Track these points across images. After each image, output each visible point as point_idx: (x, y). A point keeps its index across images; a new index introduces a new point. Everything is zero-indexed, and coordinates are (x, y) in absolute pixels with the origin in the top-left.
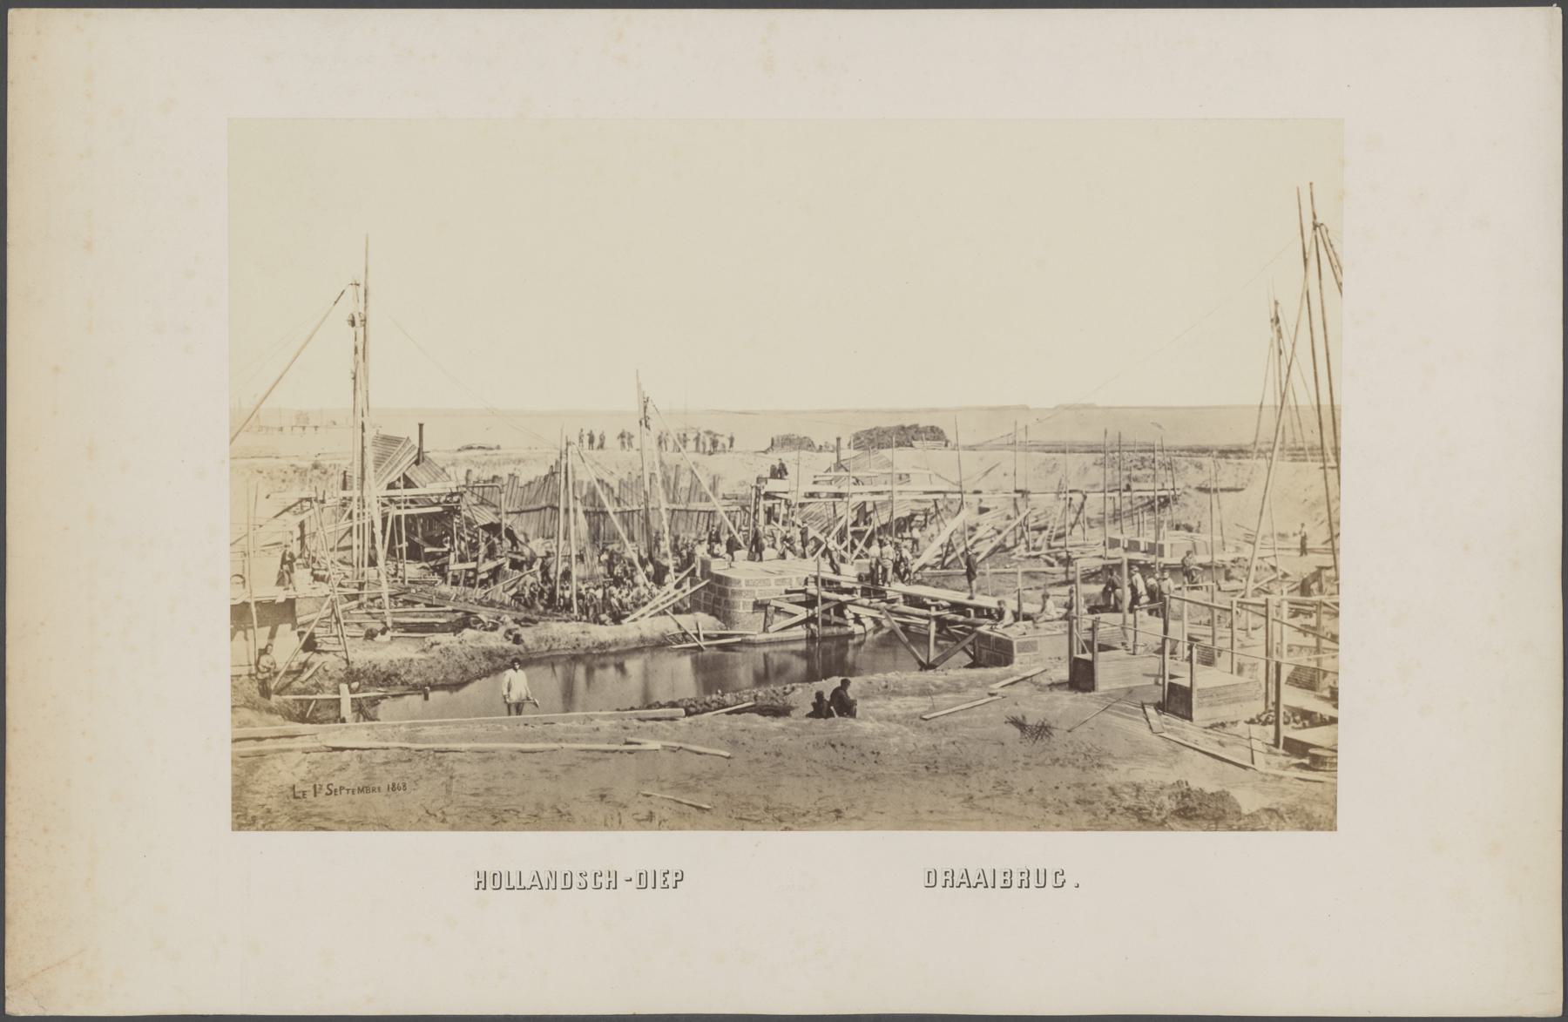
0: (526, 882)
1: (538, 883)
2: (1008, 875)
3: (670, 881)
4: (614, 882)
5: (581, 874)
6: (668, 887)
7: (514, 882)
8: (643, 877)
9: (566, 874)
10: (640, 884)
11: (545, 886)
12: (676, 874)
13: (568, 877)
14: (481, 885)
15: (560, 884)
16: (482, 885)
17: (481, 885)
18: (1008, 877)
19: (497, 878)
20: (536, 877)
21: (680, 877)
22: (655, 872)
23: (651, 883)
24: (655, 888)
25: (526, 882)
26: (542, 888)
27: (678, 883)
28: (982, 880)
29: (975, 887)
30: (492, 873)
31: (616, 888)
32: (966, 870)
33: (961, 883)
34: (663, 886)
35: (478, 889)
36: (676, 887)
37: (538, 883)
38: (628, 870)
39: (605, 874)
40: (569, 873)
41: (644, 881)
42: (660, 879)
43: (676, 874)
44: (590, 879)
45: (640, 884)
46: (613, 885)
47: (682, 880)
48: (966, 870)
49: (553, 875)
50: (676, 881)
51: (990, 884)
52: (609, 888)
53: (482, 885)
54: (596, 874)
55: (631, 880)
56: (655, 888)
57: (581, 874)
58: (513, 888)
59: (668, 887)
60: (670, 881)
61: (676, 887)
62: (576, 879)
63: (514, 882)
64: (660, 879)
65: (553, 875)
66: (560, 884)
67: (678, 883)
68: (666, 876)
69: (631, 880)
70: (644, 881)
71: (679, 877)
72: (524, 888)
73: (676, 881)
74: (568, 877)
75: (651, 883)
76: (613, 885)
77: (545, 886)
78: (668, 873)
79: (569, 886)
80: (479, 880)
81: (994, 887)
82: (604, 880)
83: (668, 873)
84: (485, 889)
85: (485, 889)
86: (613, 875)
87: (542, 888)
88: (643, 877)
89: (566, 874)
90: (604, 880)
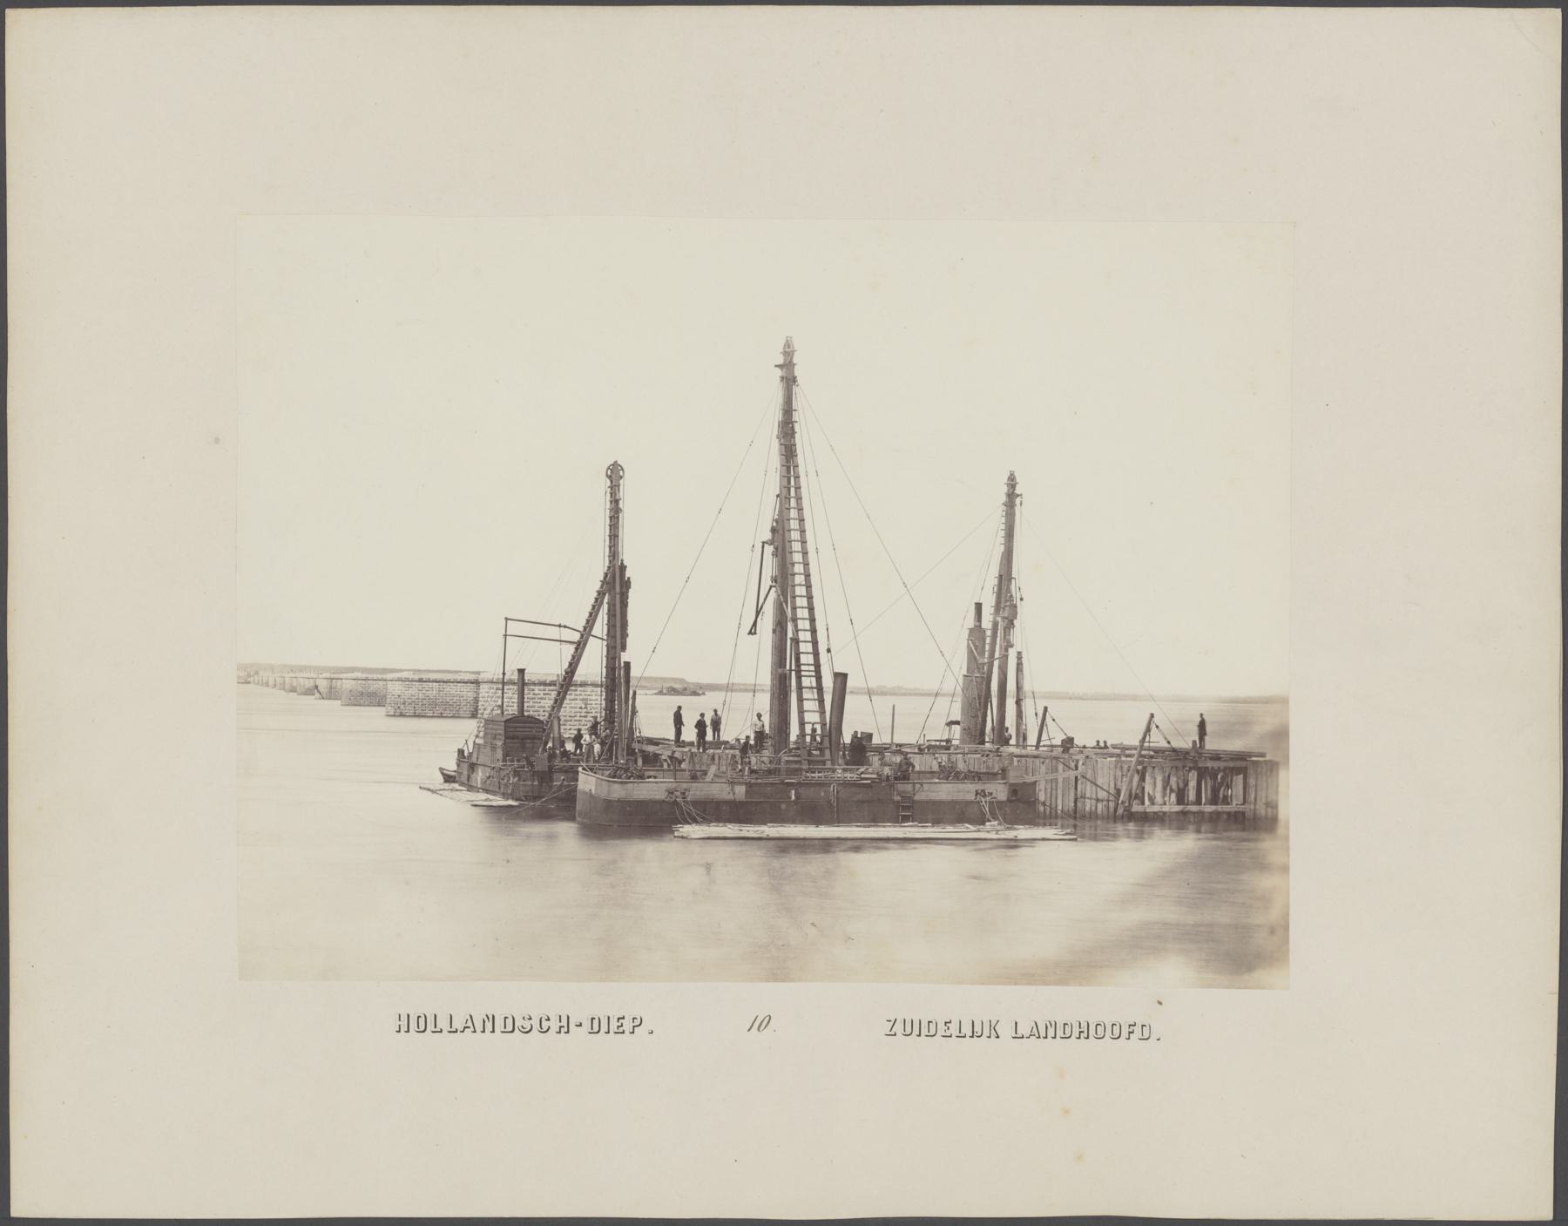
23: (604, 1028)
41: (596, 1026)
45: (592, 1029)
55: (581, 1025)
69: (581, 1025)
70: (596, 1026)
75: (604, 1028)
88: (596, 1023)
90: (554, 1024)
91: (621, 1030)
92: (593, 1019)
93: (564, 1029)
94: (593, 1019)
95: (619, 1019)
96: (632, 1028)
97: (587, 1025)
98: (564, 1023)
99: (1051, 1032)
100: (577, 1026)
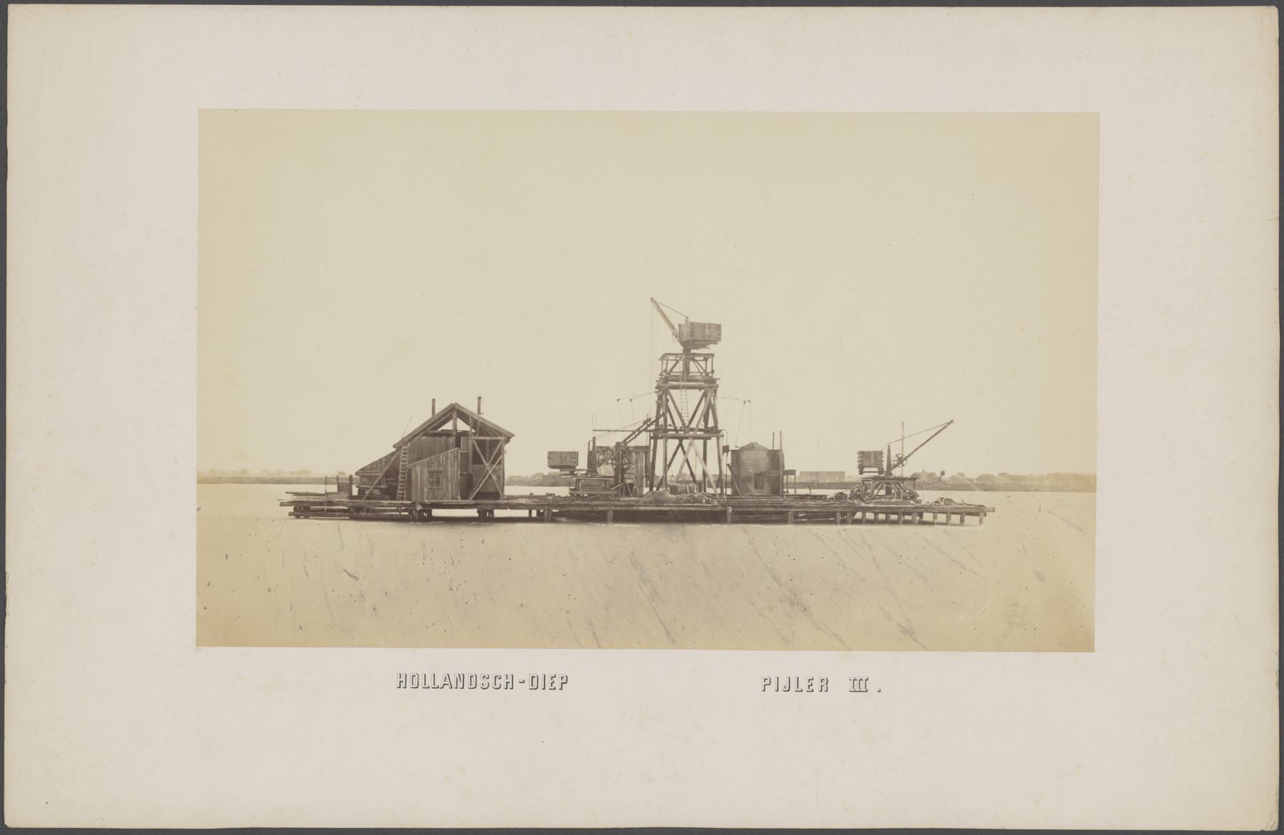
2: (825, 682)
3: (557, 685)
7: (429, 682)
9: (471, 676)
11: (454, 685)
13: (474, 679)
14: (401, 684)
16: (403, 685)
17: (401, 684)
23: (541, 685)
24: (544, 689)
25: (439, 682)
26: (452, 688)
27: (563, 685)
33: (444, 685)
37: (448, 683)
38: (522, 674)
39: (504, 678)
41: (534, 684)
44: (491, 681)
47: (566, 683)
50: (562, 683)
51: (454, 685)
52: (507, 688)
53: (403, 685)
55: (524, 682)
56: (544, 689)
59: (555, 689)
60: (557, 684)
61: (561, 689)
63: (429, 682)
65: (461, 678)
67: (563, 685)
69: (524, 682)
70: (534, 684)
73: (562, 683)
74: (474, 679)
75: (541, 685)
76: (510, 686)
78: (555, 677)
83: (555, 677)
86: (510, 678)
87: (452, 688)
88: (535, 680)
90: (503, 682)
92: (533, 677)
93: (510, 685)
94: (533, 677)
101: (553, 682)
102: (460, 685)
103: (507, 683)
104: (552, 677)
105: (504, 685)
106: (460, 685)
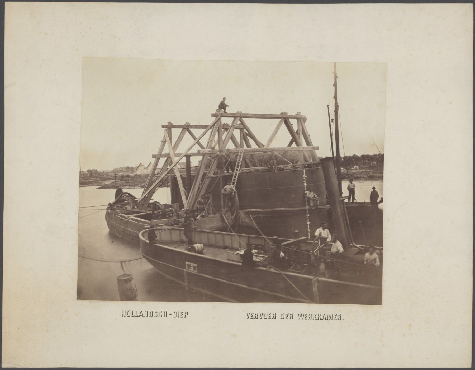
0: (138, 314)
1: (142, 315)
3: (184, 314)
4: (166, 315)
5: (155, 312)
6: (183, 317)
7: (134, 314)
8: (175, 314)
9: (151, 312)
10: (174, 316)
11: (144, 316)
12: (186, 313)
13: (151, 313)
15: (149, 315)
18: (340, 317)
19: (129, 313)
20: (141, 313)
21: (187, 314)
22: (179, 312)
23: (177, 316)
25: (138, 314)
26: (143, 316)
28: (324, 318)
29: (139, 316)
30: (174, 312)
31: (166, 317)
32: (142, 311)
34: (181, 317)
35: (123, 316)
36: (185, 317)
37: (142, 315)
38: (170, 311)
39: (163, 312)
40: (152, 312)
41: (175, 315)
42: (180, 314)
43: (186, 313)
44: (158, 314)
45: (174, 316)
46: (165, 316)
47: (187, 315)
48: (142, 311)
49: (147, 312)
50: (186, 315)
52: (164, 317)
54: (160, 312)
55: (171, 314)
56: (179, 317)
57: (155, 312)
58: (134, 316)
59: (183, 317)
60: (184, 314)
61: (185, 317)
62: (154, 314)
63: (134, 314)
64: (180, 314)
65: (147, 312)
66: (149, 315)
68: (182, 313)
70: (175, 315)
71: (187, 314)
72: (137, 316)
73: (186, 315)
74: (151, 313)
75: (177, 316)
76: (165, 316)
77: (327, 319)
79: (151, 316)
80: (165, 314)
81: (145, 317)
82: (163, 314)
83: (183, 312)
84: (125, 316)
85: (125, 316)
86: (165, 313)
87: (143, 316)
88: (175, 314)
89: (151, 312)
90: (163, 314)
91: (252, 318)
92: (174, 313)
93: (166, 316)
94: (174, 313)
95: (287, 314)
96: (290, 317)
97: (173, 314)
98: (165, 314)
99: (329, 318)
100: (170, 315)
101: (182, 315)
102: (146, 315)
103: (165, 315)
104: (182, 313)
105: (163, 316)
106: (146, 315)
